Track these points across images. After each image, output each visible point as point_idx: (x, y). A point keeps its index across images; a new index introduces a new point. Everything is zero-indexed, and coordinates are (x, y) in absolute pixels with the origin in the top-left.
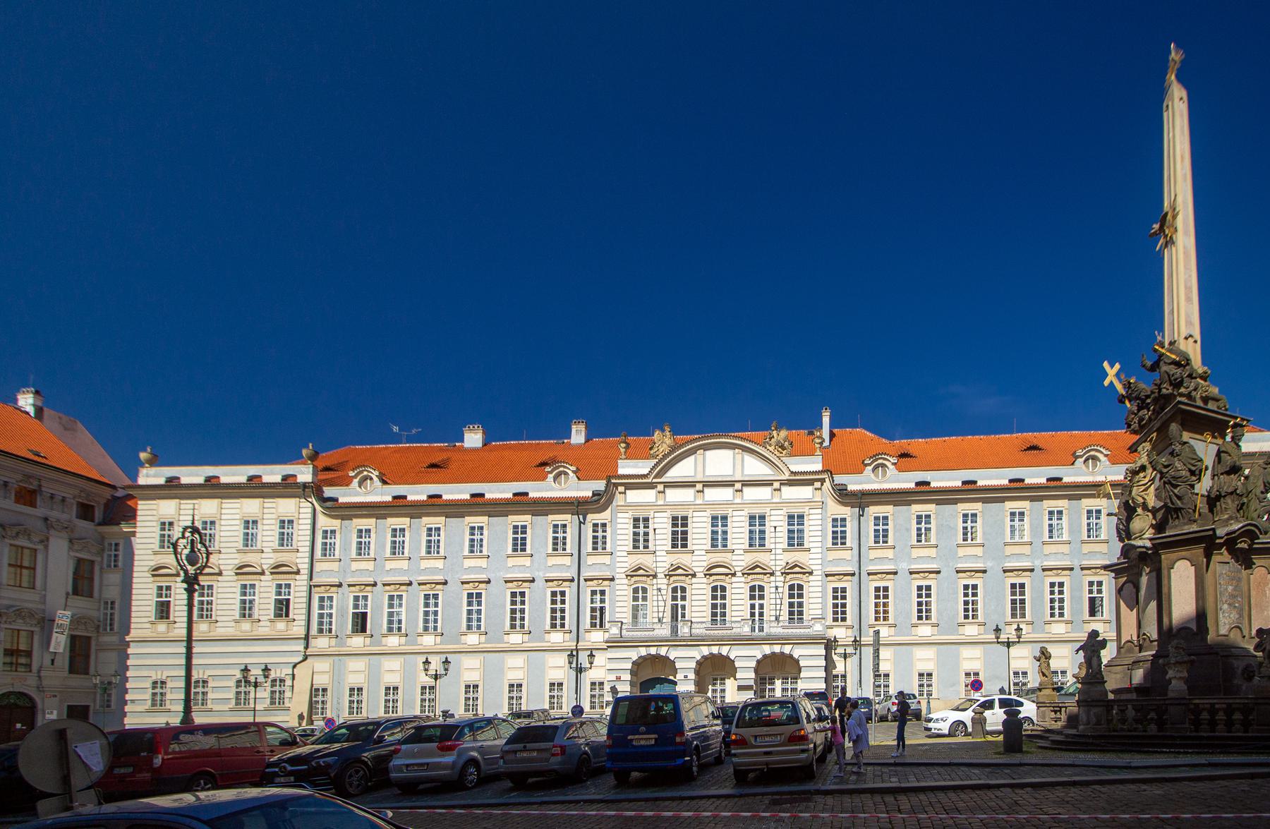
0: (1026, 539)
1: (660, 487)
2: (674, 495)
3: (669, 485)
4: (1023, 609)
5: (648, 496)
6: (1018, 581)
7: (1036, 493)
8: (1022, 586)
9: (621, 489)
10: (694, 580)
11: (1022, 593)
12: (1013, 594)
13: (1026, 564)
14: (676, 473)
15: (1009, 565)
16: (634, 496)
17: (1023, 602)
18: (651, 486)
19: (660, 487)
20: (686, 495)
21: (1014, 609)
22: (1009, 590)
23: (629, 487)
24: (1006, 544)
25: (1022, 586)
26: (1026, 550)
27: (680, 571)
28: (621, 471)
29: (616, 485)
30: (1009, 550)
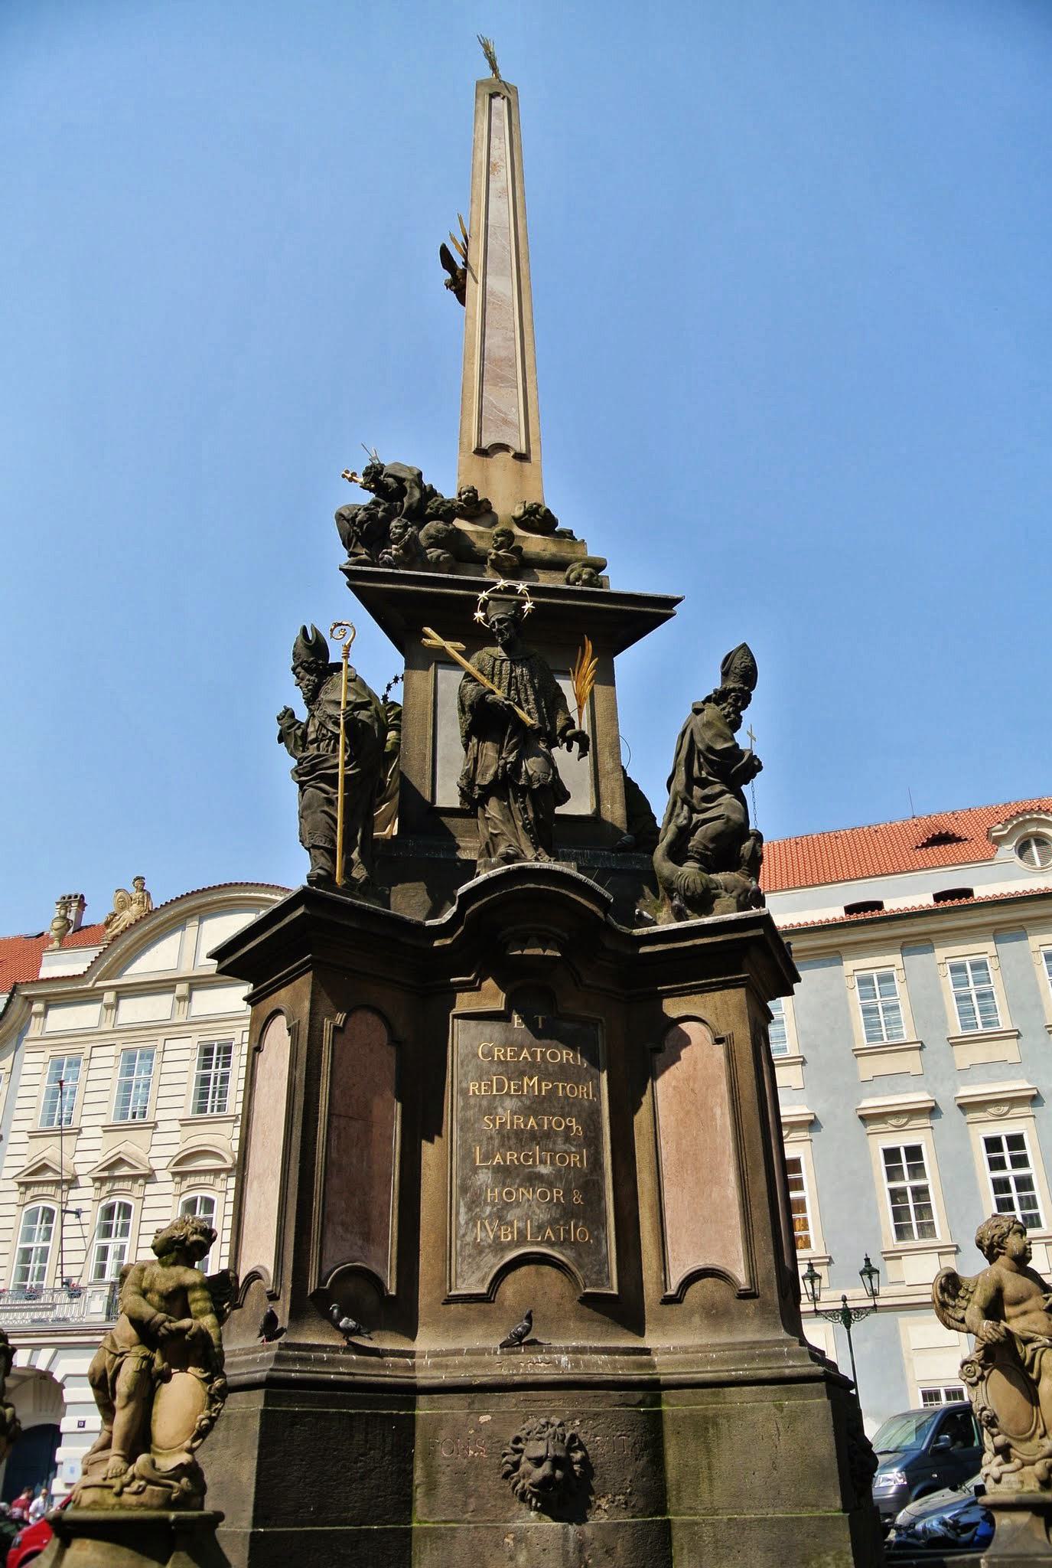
0: (908, 1035)
1: (109, 997)
2: (133, 1010)
3: (124, 992)
4: (924, 1210)
5: (87, 1015)
6: (902, 1141)
7: (912, 932)
8: (914, 1152)
9: (38, 1007)
10: (150, 1189)
11: (917, 1171)
12: (893, 1174)
13: (918, 1097)
14: (144, 967)
15: (871, 1103)
16: (62, 1019)
17: (921, 1193)
18: (91, 997)
19: (109, 997)
20: (158, 1007)
21: (899, 1214)
22: (880, 1166)
23: (53, 1002)
24: (859, 1053)
25: (914, 1152)
26: (911, 1061)
27: (124, 1171)
28: (45, 973)
29: (29, 1000)
30: (868, 1067)
